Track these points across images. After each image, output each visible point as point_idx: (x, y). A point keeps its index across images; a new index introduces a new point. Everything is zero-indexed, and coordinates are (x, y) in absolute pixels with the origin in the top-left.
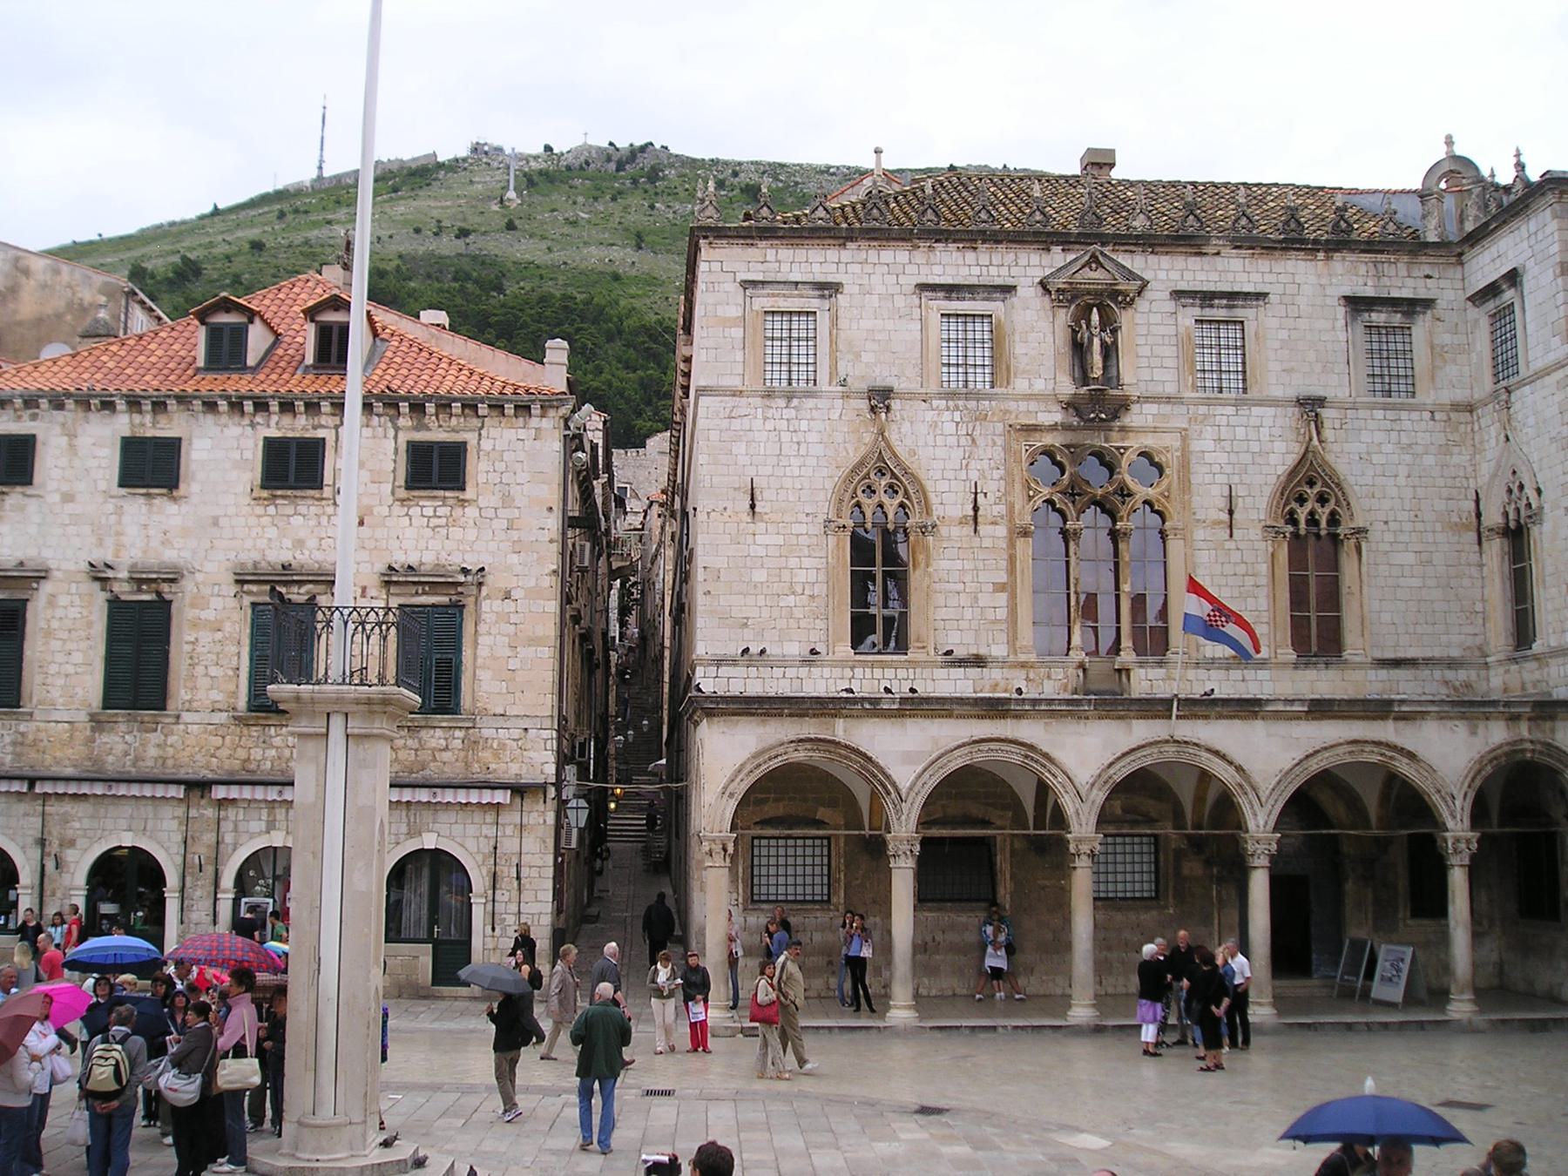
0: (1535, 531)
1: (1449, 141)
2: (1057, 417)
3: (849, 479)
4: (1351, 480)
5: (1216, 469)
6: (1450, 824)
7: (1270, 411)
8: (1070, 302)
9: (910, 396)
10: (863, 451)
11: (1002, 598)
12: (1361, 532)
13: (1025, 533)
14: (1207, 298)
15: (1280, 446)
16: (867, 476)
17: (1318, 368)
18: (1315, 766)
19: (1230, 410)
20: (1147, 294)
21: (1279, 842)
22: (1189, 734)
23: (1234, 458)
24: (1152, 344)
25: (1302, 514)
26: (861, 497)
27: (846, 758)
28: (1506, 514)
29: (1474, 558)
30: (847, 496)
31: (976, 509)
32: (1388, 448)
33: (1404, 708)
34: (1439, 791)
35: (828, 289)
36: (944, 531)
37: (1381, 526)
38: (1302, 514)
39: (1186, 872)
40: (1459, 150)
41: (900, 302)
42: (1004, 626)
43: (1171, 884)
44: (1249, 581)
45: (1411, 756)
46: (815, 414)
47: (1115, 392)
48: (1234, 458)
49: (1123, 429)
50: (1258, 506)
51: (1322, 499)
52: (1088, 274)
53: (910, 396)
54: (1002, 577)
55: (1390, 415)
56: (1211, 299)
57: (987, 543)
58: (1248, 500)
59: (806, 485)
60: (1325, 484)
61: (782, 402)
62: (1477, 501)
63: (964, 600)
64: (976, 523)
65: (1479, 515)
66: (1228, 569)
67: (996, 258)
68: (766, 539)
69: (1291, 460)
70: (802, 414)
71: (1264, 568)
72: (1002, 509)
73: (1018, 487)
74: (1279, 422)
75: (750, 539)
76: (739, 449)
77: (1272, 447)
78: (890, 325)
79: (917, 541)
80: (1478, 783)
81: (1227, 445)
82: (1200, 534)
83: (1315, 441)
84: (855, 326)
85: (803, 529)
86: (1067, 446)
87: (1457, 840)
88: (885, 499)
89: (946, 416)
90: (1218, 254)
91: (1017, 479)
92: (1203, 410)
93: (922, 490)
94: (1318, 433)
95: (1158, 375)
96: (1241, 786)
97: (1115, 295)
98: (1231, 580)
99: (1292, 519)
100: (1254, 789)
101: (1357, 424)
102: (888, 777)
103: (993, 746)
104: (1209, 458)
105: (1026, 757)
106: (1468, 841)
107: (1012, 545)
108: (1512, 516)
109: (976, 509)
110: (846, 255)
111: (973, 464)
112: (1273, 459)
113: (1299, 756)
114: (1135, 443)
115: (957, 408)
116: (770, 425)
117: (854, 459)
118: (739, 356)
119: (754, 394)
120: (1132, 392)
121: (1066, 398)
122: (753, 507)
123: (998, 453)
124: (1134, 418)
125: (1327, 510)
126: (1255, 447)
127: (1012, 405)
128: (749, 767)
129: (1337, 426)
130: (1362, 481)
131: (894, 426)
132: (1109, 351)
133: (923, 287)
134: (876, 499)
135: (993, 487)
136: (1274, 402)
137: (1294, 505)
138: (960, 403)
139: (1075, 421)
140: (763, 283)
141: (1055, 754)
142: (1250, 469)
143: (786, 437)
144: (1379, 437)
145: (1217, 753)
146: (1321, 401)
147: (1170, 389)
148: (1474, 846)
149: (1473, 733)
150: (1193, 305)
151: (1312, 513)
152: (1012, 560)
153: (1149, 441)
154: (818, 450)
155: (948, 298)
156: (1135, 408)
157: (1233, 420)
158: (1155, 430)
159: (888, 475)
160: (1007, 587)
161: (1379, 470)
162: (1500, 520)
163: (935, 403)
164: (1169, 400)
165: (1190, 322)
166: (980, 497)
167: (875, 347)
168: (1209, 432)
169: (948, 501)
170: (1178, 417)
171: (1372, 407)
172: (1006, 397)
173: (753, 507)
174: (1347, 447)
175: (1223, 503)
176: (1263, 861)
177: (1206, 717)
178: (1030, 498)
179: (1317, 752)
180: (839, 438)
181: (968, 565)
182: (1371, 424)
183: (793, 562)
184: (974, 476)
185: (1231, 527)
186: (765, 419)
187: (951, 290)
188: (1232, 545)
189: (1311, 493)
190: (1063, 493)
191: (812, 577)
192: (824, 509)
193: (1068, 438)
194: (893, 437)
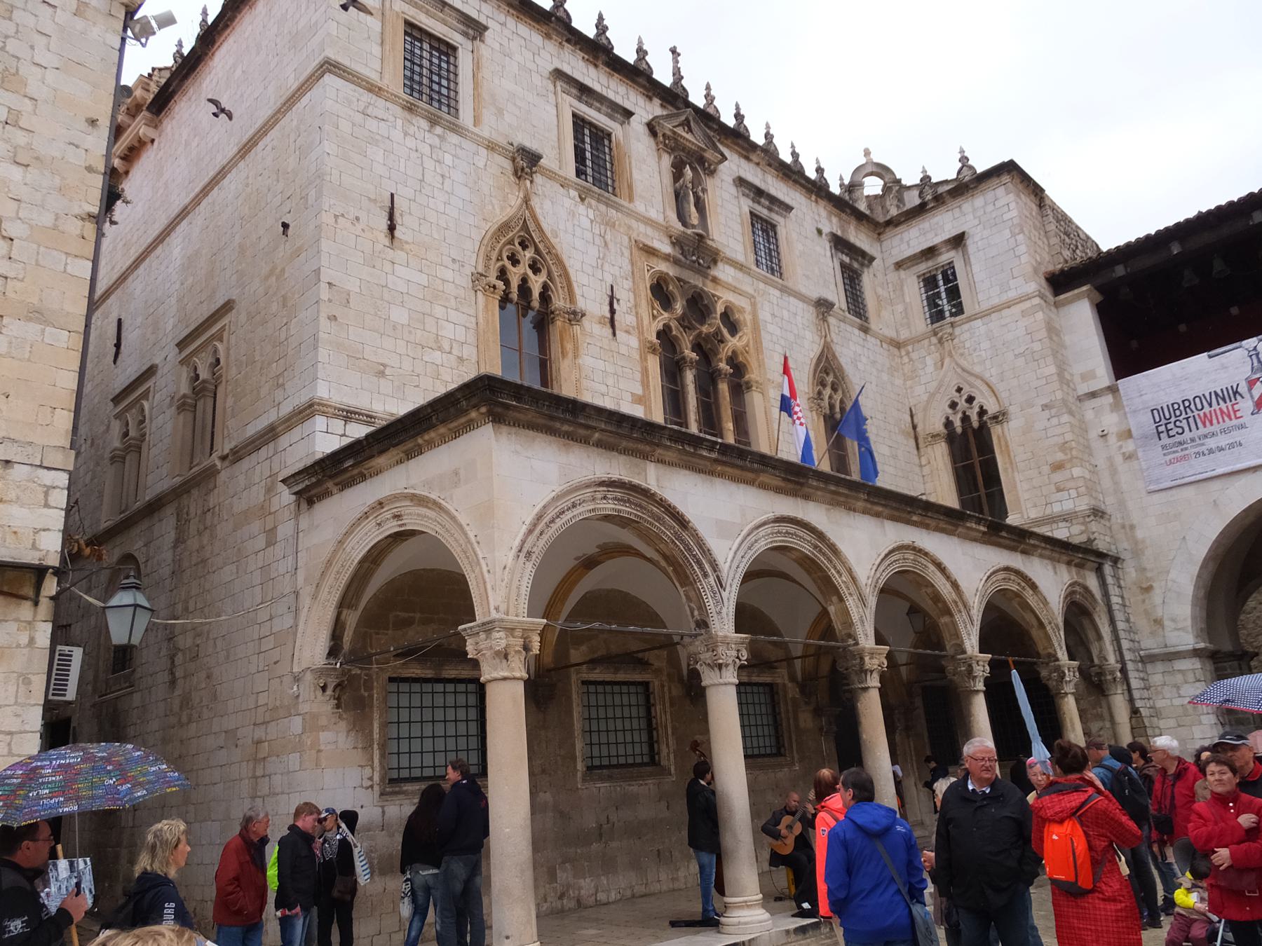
0: (996, 431)
1: (867, 153)
2: (666, 248)
8: (673, 150)
9: (551, 175)
10: (509, 212)
13: (654, 351)
14: (758, 193)
15: (808, 335)
16: (511, 242)
18: (992, 589)
19: (777, 293)
21: (991, 663)
26: (508, 264)
27: (659, 519)
28: (948, 424)
29: (916, 460)
30: (494, 256)
31: (613, 311)
39: (802, 724)
40: (876, 158)
41: (537, 80)
43: (794, 737)
45: (1034, 587)
46: (459, 151)
49: (715, 280)
51: (834, 389)
52: (680, 131)
53: (551, 175)
54: (639, 392)
57: (623, 350)
61: (424, 124)
62: (912, 416)
65: (914, 427)
68: (405, 274)
75: (388, 267)
76: (377, 154)
84: (496, 81)
85: (448, 275)
86: (679, 280)
89: (582, 209)
90: (758, 164)
92: (762, 285)
93: (566, 275)
96: (956, 602)
97: (701, 160)
102: (707, 552)
103: (791, 528)
105: (816, 547)
107: (643, 359)
108: (957, 423)
109: (613, 311)
111: (606, 266)
115: (590, 206)
116: (410, 142)
117: (501, 216)
118: (376, 50)
119: (392, 98)
122: (392, 228)
123: (627, 267)
127: (634, 223)
128: (551, 513)
132: (700, 206)
133: (558, 74)
138: (593, 202)
141: (841, 546)
143: (429, 164)
144: (859, 350)
147: (740, 258)
150: (747, 196)
152: (645, 372)
155: (580, 99)
156: (720, 265)
162: (939, 427)
165: (746, 210)
166: (616, 306)
170: (746, 284)
173: (392, 228)
176: (980, 686)
178: (654, 317)
181: (610, 369)
183: (439, 311)
184: (609, 280)
186: (406, 134)
187: (584, 91)
191: (460, 334)
192: (472, 261)
194: (538, 211)
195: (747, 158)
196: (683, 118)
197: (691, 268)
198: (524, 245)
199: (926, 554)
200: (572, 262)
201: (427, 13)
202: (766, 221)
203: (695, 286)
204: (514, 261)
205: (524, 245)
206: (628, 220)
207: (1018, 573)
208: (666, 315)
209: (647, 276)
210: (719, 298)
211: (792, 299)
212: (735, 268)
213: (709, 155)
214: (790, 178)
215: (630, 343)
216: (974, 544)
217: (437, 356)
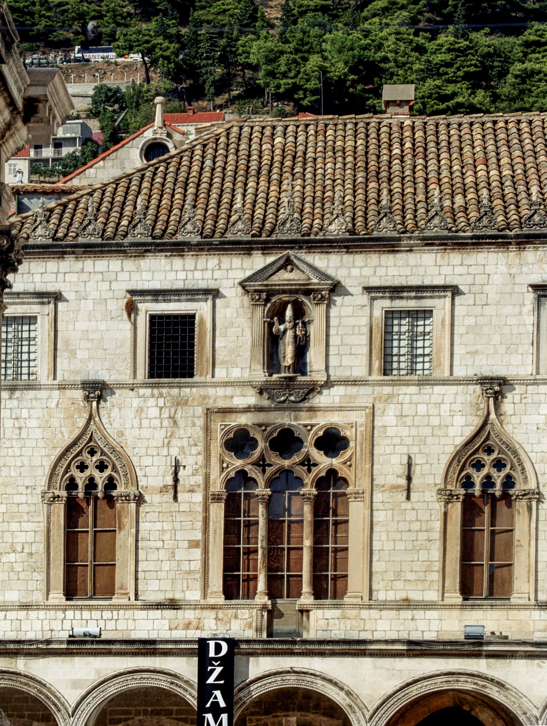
4: (527, 448)
5: (397, 441)
7: (453, 389)
15: (459, 420)
16: (80, 453)
17: (502, 349)
19: (413, 389)
23: (414, 431)
31: (176, 480)
47: (301, 378)
48: (414, 431)
49: (312, 409)
50: (433, 471)
59: (26, 462)
64: (176, 492)
72: (199, 479)
74: (460, 399)
79: (123, 508)
86: (260, 425)
88: (96, 474)
91: (213, 453)
93: (129, 466)
95: (346, 361)
101: (536, 398)
104: (390, 432)
109: (176, 480)
112: (452, 431)
114: (322, 421)
120: (321, 378)
126: (435, 421)
134: (87, 473)
135: (192, 460)
139: (265, 403)
142: (429, 440)
146: (503, 382)
157: (415, 398)
159: (99, 454)
168: (392, 410)
169: (152, 474)
174: (525, 419)
184: (174, 452)
190: (254, 464)
193: (261, 418)
197: (276, 409)
200: (136, 451)
203: (281, 425)
210: (312, 426)
211: (437, 389)
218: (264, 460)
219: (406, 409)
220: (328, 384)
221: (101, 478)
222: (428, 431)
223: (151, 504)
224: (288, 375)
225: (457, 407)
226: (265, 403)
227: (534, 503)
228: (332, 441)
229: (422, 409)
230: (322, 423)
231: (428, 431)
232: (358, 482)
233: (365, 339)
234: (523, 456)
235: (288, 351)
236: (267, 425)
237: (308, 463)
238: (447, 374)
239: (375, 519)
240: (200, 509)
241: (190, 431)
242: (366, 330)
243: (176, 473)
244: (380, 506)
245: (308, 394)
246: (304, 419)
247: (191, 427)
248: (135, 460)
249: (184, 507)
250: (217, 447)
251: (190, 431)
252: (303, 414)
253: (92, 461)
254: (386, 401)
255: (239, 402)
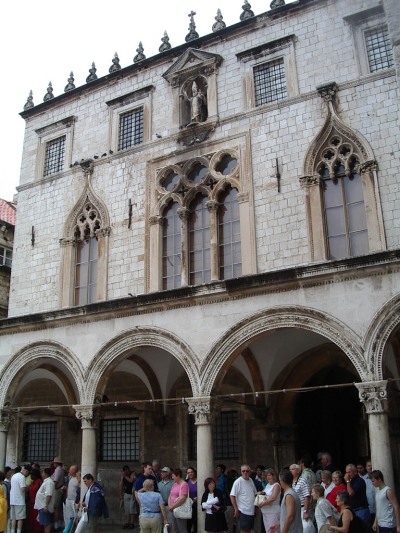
2: (174, 147)
3: (70, 215)
4: (363, 131)
6: (363, 375)
11: (142, 264)
12: (372, 165)
13: (154, 221)
14: (256, 52)
16: (82, 211)
18: (241, 336)
19: (276, 112)
20: (225, 64)
22: (150, 323)
24: (229, 89)
25: (330, 164)
31: (130, 215)
32: (388, 103)
33: (305, 276)
34: (349, 346)
35: (69, 121)
36: (114, 231)
37: (389, 157)
38: (330, 164)
39: (255, 438)
42: (143, 281)
44: (293, 219)
45: (321, 316)
48: (279, 141)
52: (190, 65)
54: (142, 251)
55: (387, 80)
56: (260, 51)
58: (290, 165)
60: (345, 140)
63: (123, 269)
66: (279, 214)
67: (147, 76)
68: (38, 255)
69: (318, 131)
70: (57, 187)
71: (303, 208)
72: (143, 211)
73: (153, 195)
74: (309, 109)
77: (302, 125)
78: (95, 129)
80: (388, 332)
81: (275, 135)
82: (259, 195)
83: (333, 114)
85: (51, 247)
86: (178, 164)
87: (368, 389)
90: (264, 26)
92: (259, 117)
93: (105, 211)
94: (336, 107)
98: (281, 222)
99: (323, 169)
100: (194, 361)
103: (41, 348)
106: (377, 389)
107: (147, 230)
109: (130, 215)
110: (80, 102)
113: (226, 329)
114: (217, 150)
117: (75, 202)
121: (176, 137)
122: (33, 240)
124: (217, 136)
125: (348, 157)
126: (293, 130)
127: (151, 150)
129: (350, 98)
130: (369, 131)
131: (94, 181)
133: (109, 103)
135: (139, 200)
136: (304, 98)
137: (323, 160)
138: (126, 158)
139: (183, 148)
140: (43, 128)
143: (49, 201)
144: (380, 97)
145: (167, 336)
147: (237, 112)
148: (384, 393)
149: (378, 287)
150: (250, 60)
151: (338, 163)
153: (226, 146)
154: (61, 204)
155: (122, 105)
156: (218, 129)
158: (229, 138)
160: (146, 258)
161: (383, 119)
163: (114, 162)
164: (236, 118)
166: (134, 208)
167: (88, 142)
168: (263, 129)
169: (116, 213)
170: (242, 126)
171: (374, 79)
172: (147, 147)
173: (33, 240)
174: (358, 111)
175: (273, 171)
177: (160, 309)
179: (240, 325)
180: (70, 194)
182: (374, 91)
184: (130, 196)
185: (279, 186)
187: (121, 100)
188: (281, 197)
189: (335, 148)
193: (180, 159)
195: (254, 30)
196: (186, 56)
198: (88, 209)
199: (154, 331)
201: (53, 132)
202: (274, 62)
203: (192, 160)
204: (83, 219)
205: (88, 209)
206: (146, 152)
207: (291, 310)
208: (166, 193)
209: (156, 176)
210: (212, 155)
211: (292, 107)
212: (232, 122)
213: (207, 62)
214: (299, 9)
215: (139, 226)
216: (223, 304)
217: (45, 287)
218: (183, 188)
219: (273, 127)
220: (219, 124)
221: (91, 223)
222: (289, 137)
223: (117, 235)
224: (195, 128)
225: (307, 116)
226: (183, 148)
227: (375, 173)
228: (225, 161)
229: (283, 123)
230: (217, 151)
231: (289, 137)
232: (244, 187)
233: (241, 89)
234: (361, 139)
235: (195, 109)
236: (183, 163)
237: (211, 182)
238: (297, 93)
239: (257, 213)
240: (143, 231)
241: (139, 180)
242: (240, 83)
243: (131, 209)
244: (261, 202)
245: (207, 134)
246: (207, 151)
247: (139, 178)
248: (109, 207)
249: (135, 233)
250: (155, 185)
251: (139, 180)
252: (206, 149)
253: (87, 214)
254: (258, 125)
255: (167, 152)
